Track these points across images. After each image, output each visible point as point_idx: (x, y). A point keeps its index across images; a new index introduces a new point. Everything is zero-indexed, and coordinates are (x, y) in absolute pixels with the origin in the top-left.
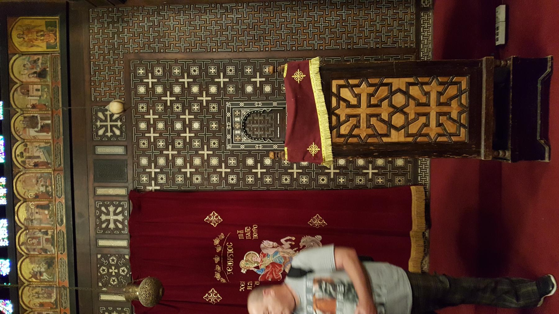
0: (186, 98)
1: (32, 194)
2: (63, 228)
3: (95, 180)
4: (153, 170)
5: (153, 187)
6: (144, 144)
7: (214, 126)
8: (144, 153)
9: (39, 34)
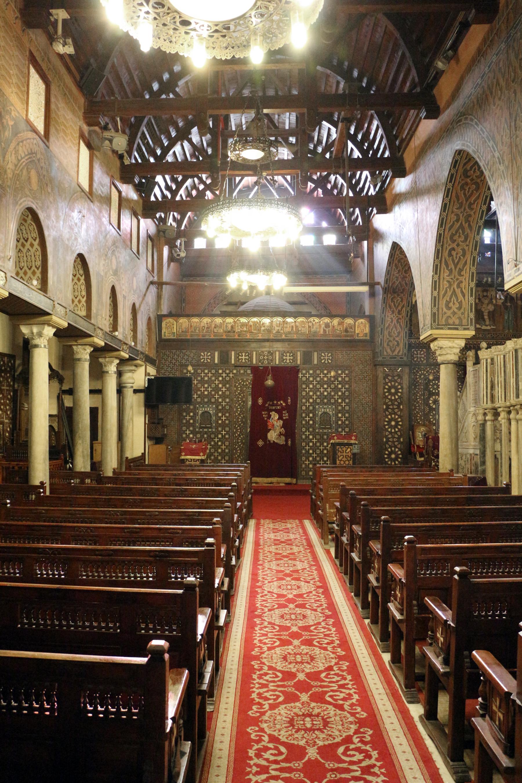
0: (336, 390)
1: (297, 324)
2: (283, 337)
3: (304, 351)
4: (307, 375)
5: (300, 375)
6: (318, 372)
7: (325, 401)
8: (315, 372)
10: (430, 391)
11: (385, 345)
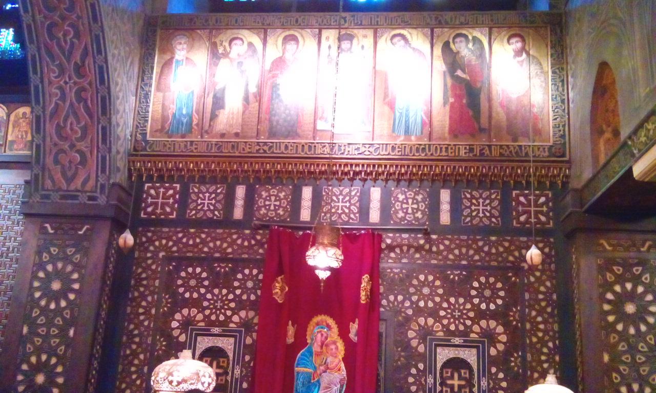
9: (24, 134)
10: (174, 294)
11: (49, 161)
